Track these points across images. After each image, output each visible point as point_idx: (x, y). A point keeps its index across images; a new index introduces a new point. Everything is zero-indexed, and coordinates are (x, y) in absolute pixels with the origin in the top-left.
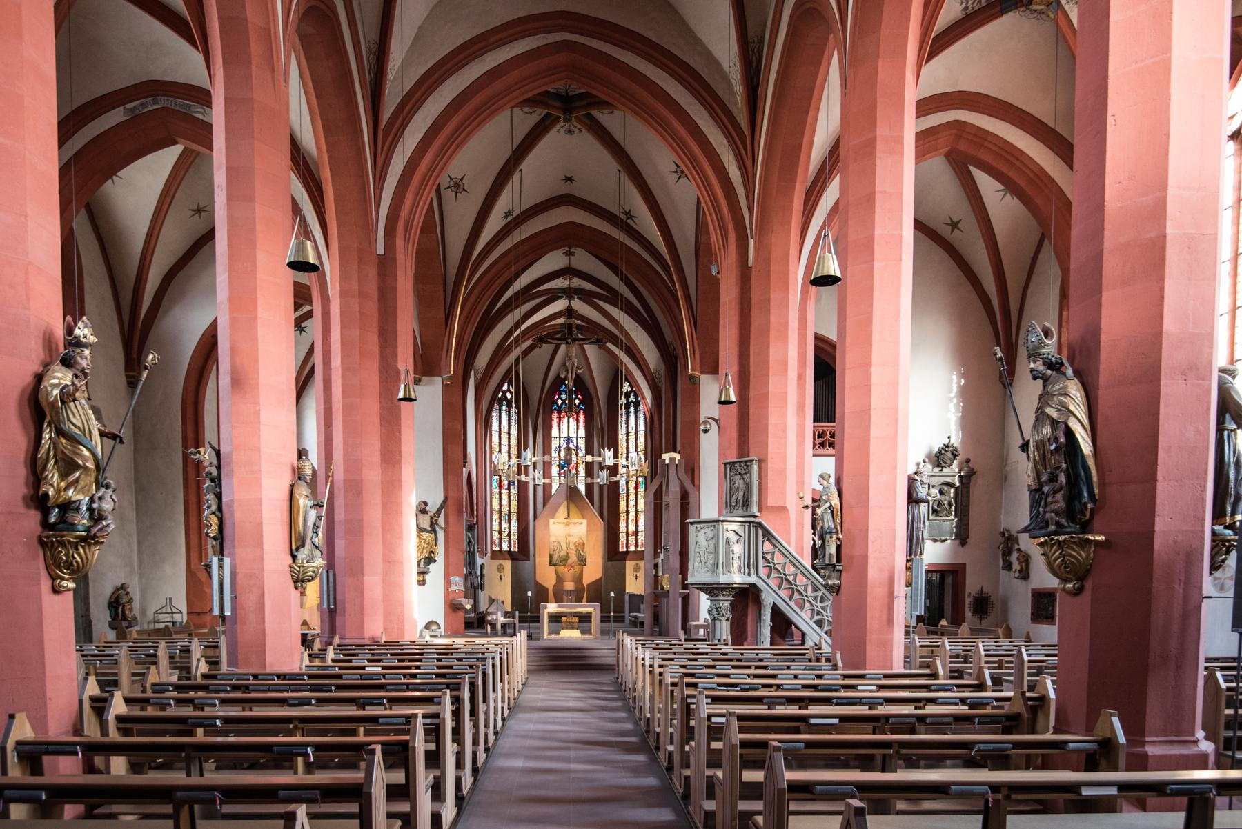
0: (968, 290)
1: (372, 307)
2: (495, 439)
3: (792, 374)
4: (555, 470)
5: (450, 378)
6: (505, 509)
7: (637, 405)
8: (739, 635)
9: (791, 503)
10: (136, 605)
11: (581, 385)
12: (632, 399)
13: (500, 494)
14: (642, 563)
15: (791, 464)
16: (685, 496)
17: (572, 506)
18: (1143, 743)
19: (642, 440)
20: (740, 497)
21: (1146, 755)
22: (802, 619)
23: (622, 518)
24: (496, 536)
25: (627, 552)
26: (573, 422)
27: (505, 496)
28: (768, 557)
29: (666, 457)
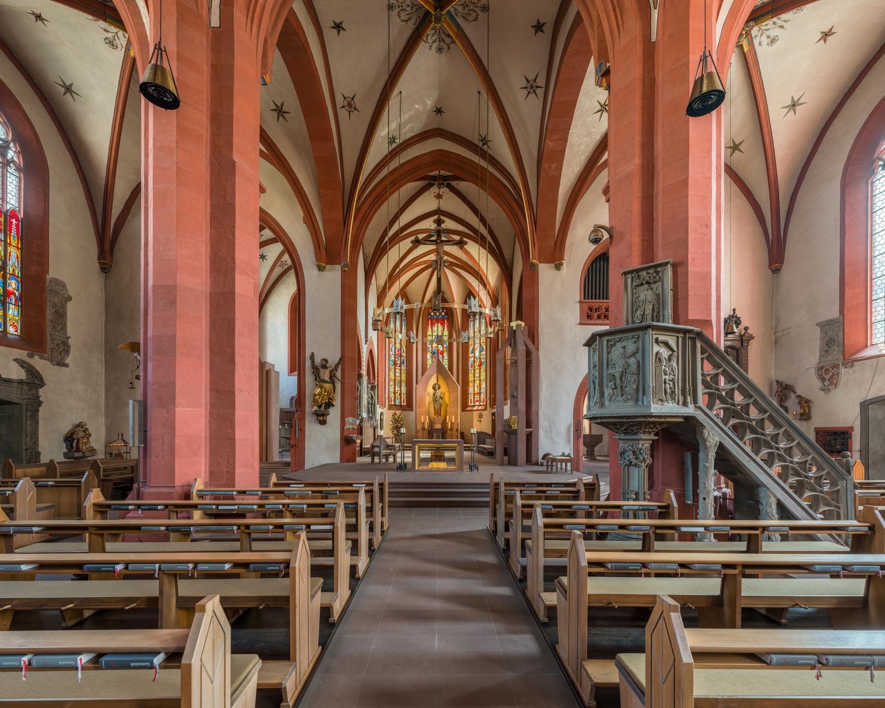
4: (429, 356)
14: (484, 413)
16: (528, 354)
17: (440, 377)
23: (471, 384)
24: (392, 395)
26: (440, 328)
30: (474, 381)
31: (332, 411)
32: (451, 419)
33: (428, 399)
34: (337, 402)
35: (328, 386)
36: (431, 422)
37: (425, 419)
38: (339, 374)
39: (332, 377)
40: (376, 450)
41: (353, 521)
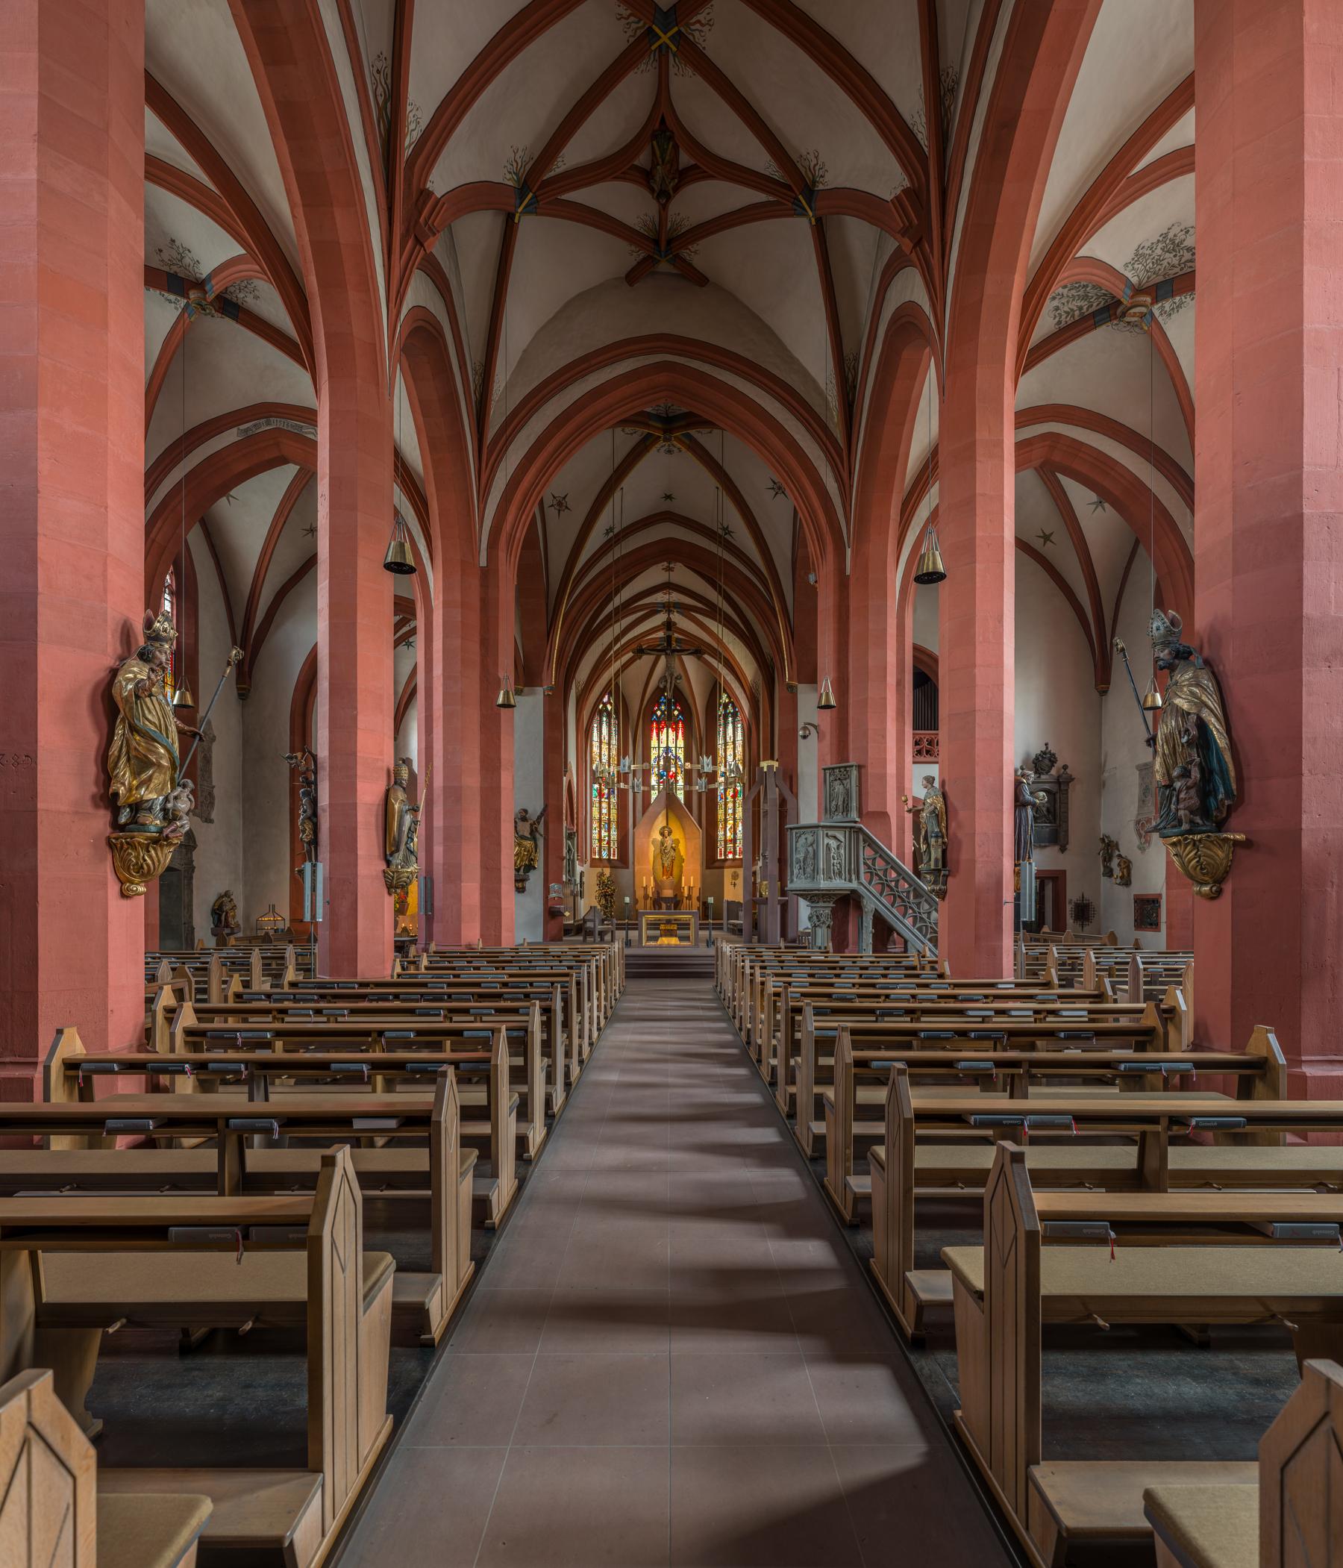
0: (1060, 601)
1: (475, 618)
2: (596, 750)
3: (891, 679)
5: (551, 689)
6: (605, 818)
7: (734, 715)
8: (840, 942)
9: (891, 808)
10: (240, 912)
11: (680, 698)
12: (730, 709)
13: (600, 803)
14: (740, 871)
15: (891, 769)
16: (783, 802)
18: (1301, 1063)
19: (739, 749)
20: (840, 803)
21: (1303, 1077)
22: (905, 925)
24: (596, 844)
25: (726, 860)
26: (672, 735)
27: (604, 805)
28: (869, 863)
29: (764, 765)
30: (726, 821)
31: (532, 874)
32: (688, 881)
33: (652, 850)
34: (539, 864)
35: (528, 844)
36: (658, 887)
37: (648, 881)
38: (541, 828)
39: (533, 832)
40: (589, 925)
41: (519, 1061)
